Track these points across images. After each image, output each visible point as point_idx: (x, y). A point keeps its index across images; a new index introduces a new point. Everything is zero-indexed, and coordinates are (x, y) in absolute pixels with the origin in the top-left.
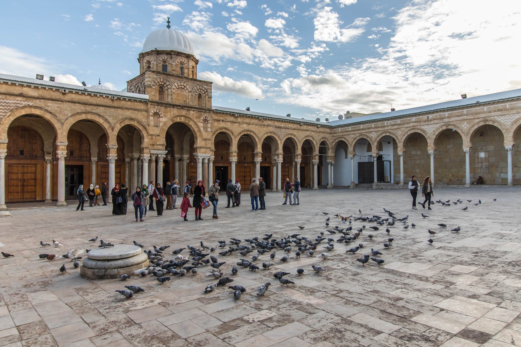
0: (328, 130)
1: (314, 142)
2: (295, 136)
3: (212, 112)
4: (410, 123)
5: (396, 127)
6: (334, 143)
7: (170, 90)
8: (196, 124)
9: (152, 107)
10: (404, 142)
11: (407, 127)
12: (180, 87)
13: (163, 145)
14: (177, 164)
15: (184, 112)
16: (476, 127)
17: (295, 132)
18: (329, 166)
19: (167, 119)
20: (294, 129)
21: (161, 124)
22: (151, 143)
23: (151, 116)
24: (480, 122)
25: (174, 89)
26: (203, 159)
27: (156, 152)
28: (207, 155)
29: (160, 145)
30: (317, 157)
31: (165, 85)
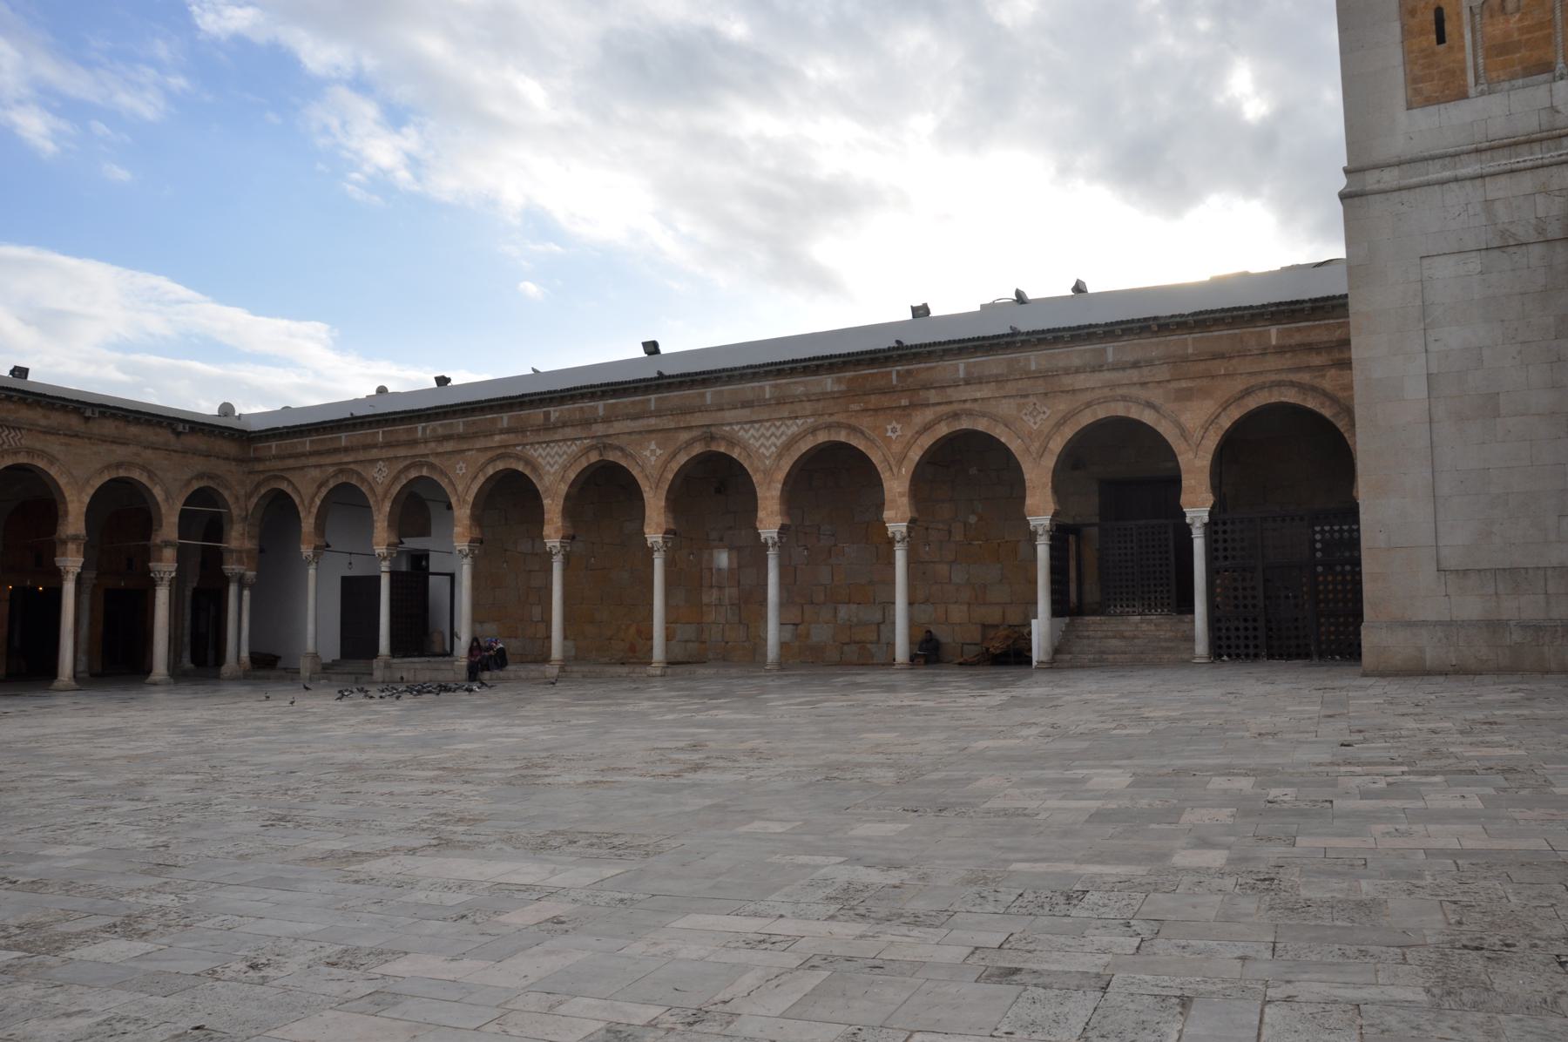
0: (230, 448)
1: (158, 492)
2: (52, 460)
4: (492, 435)
5: (449, 446)
6: (255, 500)
10: (474, 505)
11: (486, 449)
16: (683, 459)
17: (54, 446)
18: (233, 589)
20: (49, 431)
24: (693, 441)
30: (169, 553)
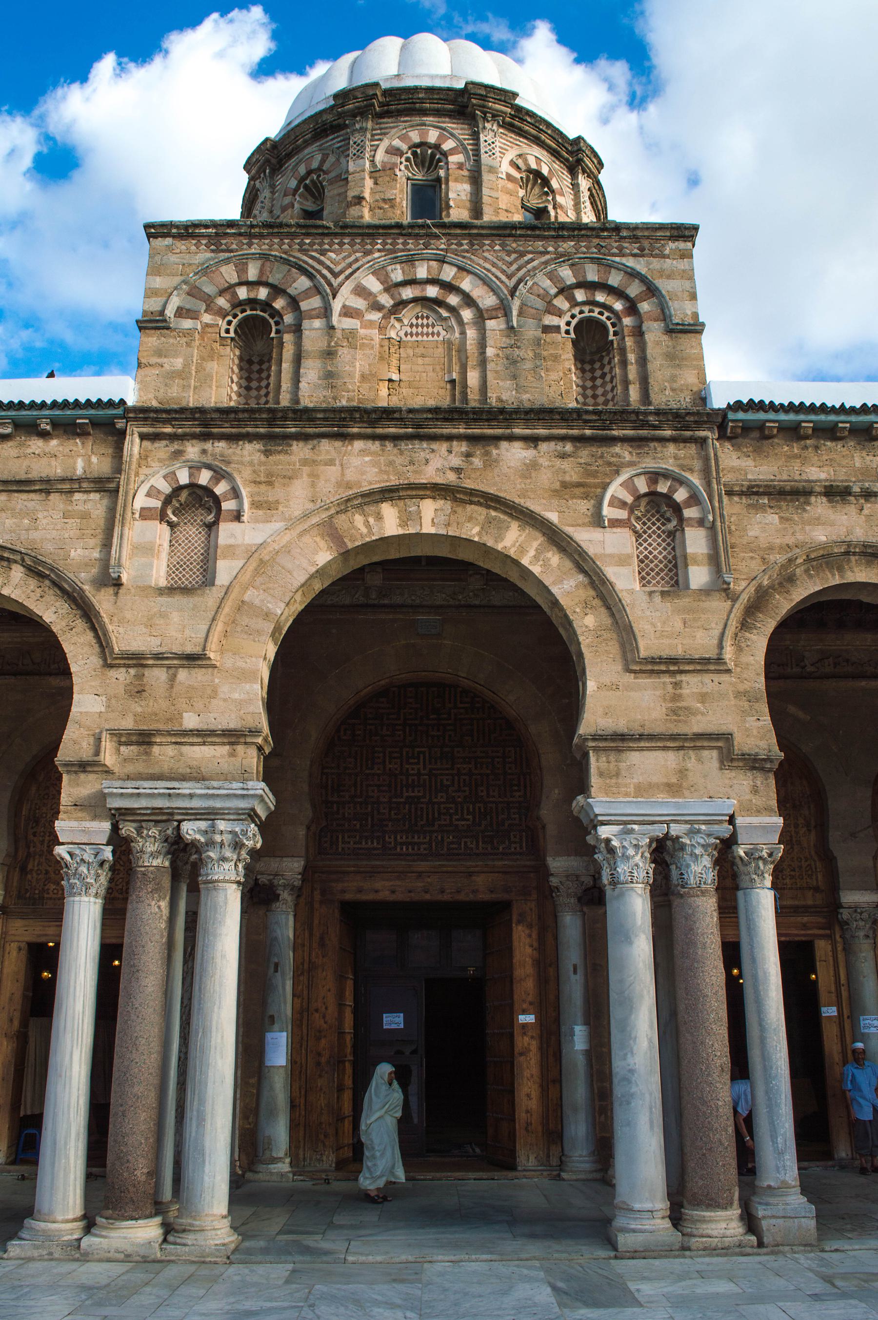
3: (710, 435)
7: (317, 323)
8: (556, 538)
9: (161, 449)
12: (408, 293)
13: (233, 737)
14: (571, 925)
15: (438, 462)
19: (286, 535)
21: (225, 571)
22: (128, 723)
23: (146, 514)
25: (347, 312)
26: (664, 852)
27: (150, 795)
28: (695, 805)
29: (204, 735)
31: (279, 304)
